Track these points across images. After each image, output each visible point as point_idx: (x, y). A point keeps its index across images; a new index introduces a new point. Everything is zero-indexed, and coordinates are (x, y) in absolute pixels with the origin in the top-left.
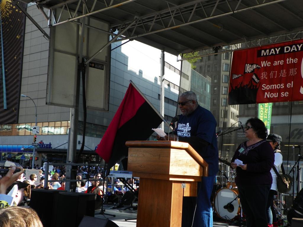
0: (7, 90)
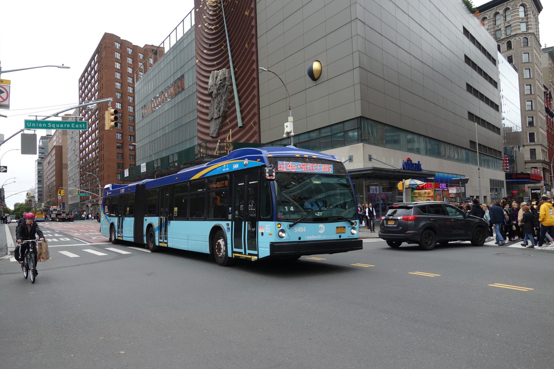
0: (240, 98)
